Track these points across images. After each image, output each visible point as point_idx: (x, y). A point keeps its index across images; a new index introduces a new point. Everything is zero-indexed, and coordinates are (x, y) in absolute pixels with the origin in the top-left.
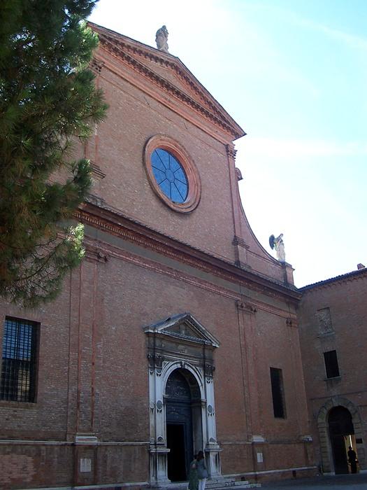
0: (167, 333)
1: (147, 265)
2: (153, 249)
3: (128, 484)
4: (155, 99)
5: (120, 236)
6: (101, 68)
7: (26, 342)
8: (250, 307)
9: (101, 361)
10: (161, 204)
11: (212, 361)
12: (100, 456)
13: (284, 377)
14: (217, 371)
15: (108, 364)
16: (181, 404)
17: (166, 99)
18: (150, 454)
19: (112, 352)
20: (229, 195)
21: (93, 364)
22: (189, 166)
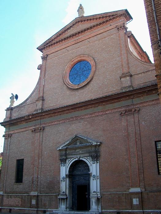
3: (49, 209)
5: (49, 117)
12: (39, 199)
17: (75, 40)
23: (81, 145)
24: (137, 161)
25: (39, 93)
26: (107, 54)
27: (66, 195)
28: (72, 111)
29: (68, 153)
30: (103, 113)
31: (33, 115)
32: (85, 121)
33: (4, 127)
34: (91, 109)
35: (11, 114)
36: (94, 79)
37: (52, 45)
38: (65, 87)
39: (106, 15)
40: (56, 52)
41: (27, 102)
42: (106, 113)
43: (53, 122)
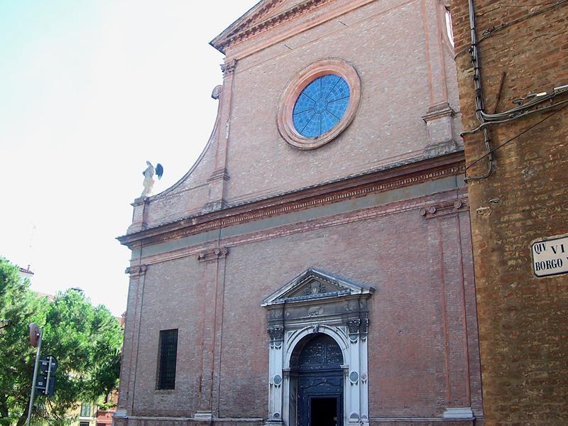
1: (270, 235)
2: (278, 214)
5: (241, 223)
17: (308, 21)
19: (231, 336)
23: (322, 295)
24: (465, 340)
25: (217, 162)
26: (391, 58)
27: (282, 421)
28: (300, 208)
29: (288, 314)
30: (379, 213)
31: (200, 217)
32: (333, 234)
33: (129, 248)
34: (348, 200)
35: (145, 213)
36: (356, 124)
37: (248, 33)
38: (282, 145)
40: (257, 52)
41: (187, 182)
42: (388, 211)
43: (252, 235)
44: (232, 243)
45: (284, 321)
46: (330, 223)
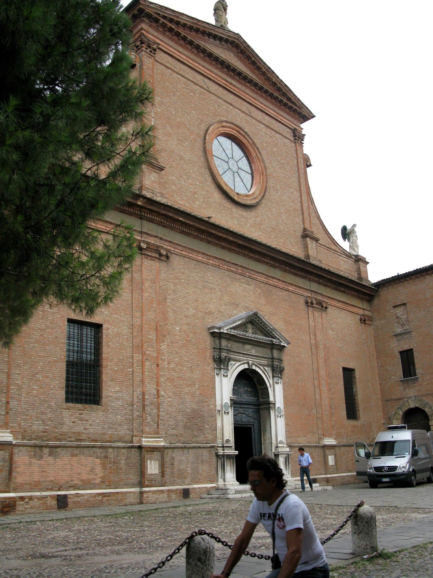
0: (233, 332)
1: (211, 262)
3: (196, 486)
4: (214, 82)
6: (155, 50)
7: (89, 344)
8: (320, 303)
9: (166, 363)
10: (224, 197)
11: (280, 360)
12: (167, 459)
13: (357, 377)
14: (286, 371)
15: (172, 365)
16: (250, 406)
18: (217, 456)
19: (177, 353)
20: (296, 184)
21: (158, 365)
22: (253, 154)
39: (286, 90)
42: (289, 288)
44: (173, 249)
45: (220, 349)
46: (256, 277)
